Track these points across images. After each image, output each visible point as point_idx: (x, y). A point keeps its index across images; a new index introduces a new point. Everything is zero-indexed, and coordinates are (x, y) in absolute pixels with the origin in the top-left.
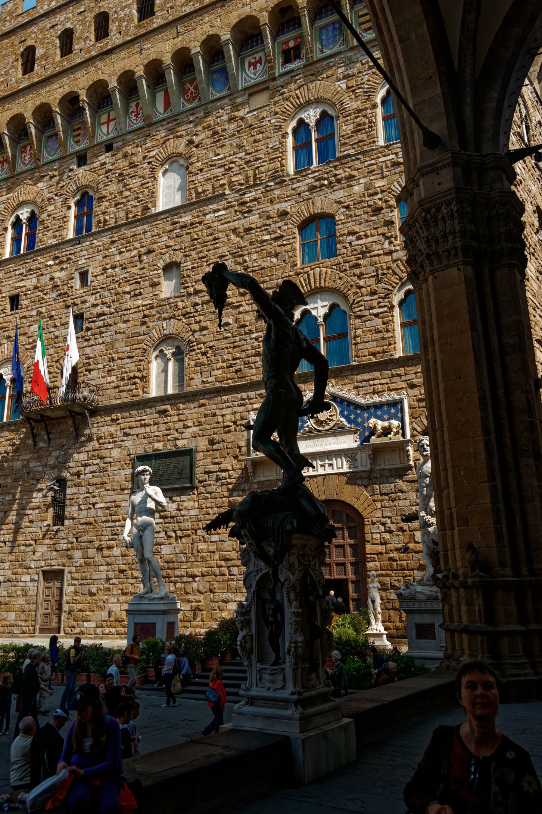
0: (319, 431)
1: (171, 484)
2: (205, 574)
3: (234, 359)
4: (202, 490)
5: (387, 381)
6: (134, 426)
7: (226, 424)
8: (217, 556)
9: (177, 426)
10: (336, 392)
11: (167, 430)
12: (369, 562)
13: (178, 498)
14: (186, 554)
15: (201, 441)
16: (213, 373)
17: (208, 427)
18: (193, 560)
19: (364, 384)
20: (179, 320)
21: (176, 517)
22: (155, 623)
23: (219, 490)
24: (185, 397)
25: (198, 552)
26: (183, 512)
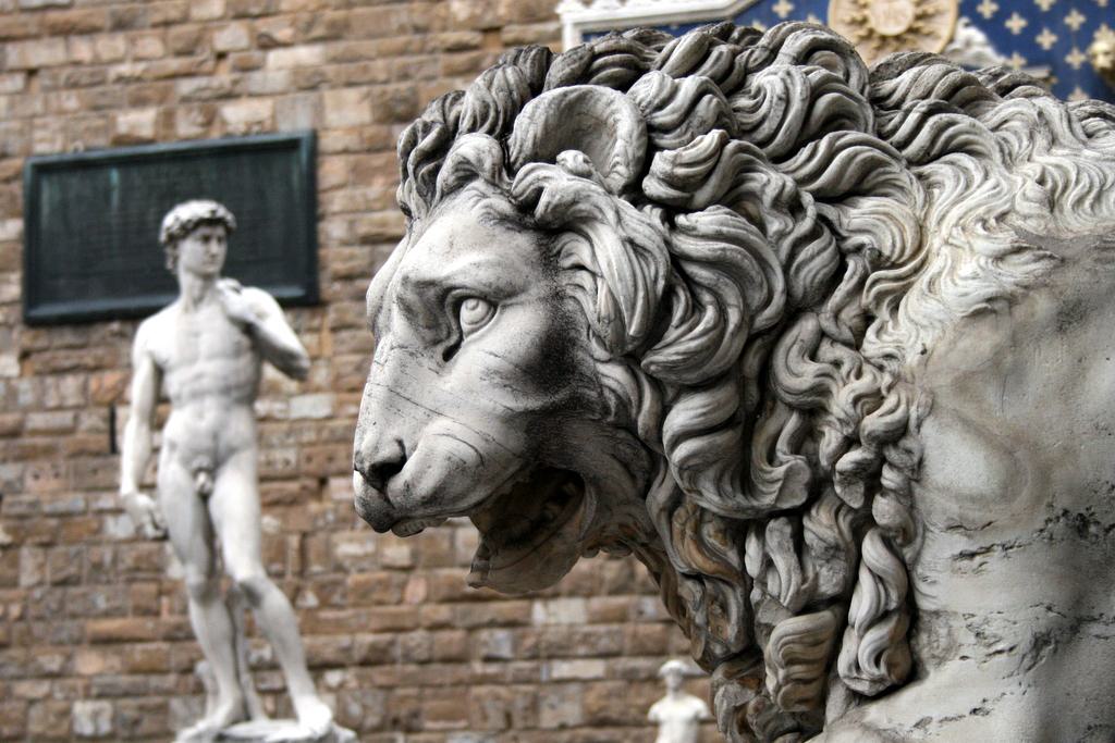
6: (19, 31)
11: (179, 54)
15: (339, 106)
17: (368, 47)
25: (340, 568)
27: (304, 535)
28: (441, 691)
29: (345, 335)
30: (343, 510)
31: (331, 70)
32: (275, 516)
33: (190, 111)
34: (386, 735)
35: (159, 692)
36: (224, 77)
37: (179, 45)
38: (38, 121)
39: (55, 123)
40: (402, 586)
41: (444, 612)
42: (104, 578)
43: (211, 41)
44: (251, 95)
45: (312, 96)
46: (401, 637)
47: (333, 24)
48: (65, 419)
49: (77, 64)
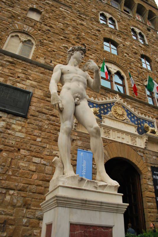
0: (116, 118)
1: (5, 107)
4: (33, 121)
5: (146, 111)
9: (20, 75)
12: (148, 202)
13: (8, 120)
14: (4, 166)
15: (38, 91)
16: (53, 62)
18: (10, 173)
19: (137, 108)
20: (36, 30)
22: (111, 228)
23: (47, 127)
24: (30, 63)
25: (19, 168)
26: (9, 132)
27: (12, 159)
28: (36, 200)
29: (31, 125)
30: (22, 156)
31: (38, 86)
32: (6, 154)
34: (21, 208)
36: (18, 80)
37: (12, 72)
40: (32, 175)
41: (41, 183)
43: (18, 74)
44: (22, 84)
45: (34, 88)
46: (30, 186)
47: (40, 81)
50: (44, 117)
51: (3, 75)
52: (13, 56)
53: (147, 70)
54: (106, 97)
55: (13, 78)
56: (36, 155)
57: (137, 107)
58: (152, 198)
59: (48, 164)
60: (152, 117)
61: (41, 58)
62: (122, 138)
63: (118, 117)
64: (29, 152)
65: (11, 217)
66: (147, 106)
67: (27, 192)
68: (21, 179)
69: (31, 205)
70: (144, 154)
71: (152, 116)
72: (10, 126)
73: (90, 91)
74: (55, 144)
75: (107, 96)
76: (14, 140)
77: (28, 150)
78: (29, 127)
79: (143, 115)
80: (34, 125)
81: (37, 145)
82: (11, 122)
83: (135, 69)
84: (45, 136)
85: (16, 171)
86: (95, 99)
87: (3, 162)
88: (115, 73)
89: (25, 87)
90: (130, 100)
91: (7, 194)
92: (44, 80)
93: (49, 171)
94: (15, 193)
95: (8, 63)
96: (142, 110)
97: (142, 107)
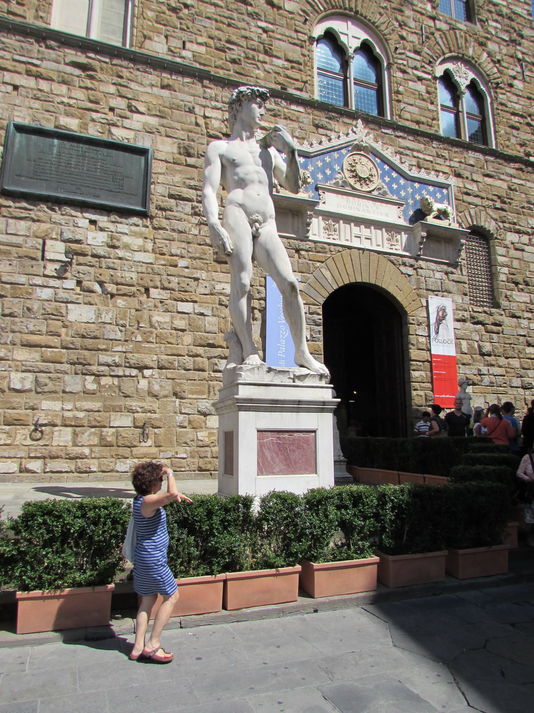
0: (354, 188)
1: (98, 197)
2: (167, 365)
3: (229, 42)
4: (164, 223)
6: (10, 68)
7: (212, 132)
8: (188, 338)
10: (378, 149)
11: (91, 101)
12: (414, 370)
13: (112, 227)
14: (123, 326)
15: (163, 143)
16: (188, 45)
18: (139, 338)
19: (408, 152)
21: (105, 257)
23: (197, 232)
24: (131, 60)
25: (152, 326)
26: (120, 253)
31: (162, 129)
33: (96, 126)
35: (57, 371)
37: (92, 98)
38: (16, 108)
39: (25, 112)
42: (33, 316)
43: (107, 102)
48: (19, 240)
49: (41, 90)
50: (187, 207)
51: (72, 110)
52: (84, 45)
53: (450, 24)
54: (329, 133)
55: (99, 115)
56: (183, 297)
57: (409, 149)
58: (423, 362)
59: (209, 313)
60: (444, 173)
61: (156, 38)
62: (366, 238)
63: (358, 186)
64: (169, 291)
65: (154, 416)
66: (435, 144)
67: (175, 369)
68: (160, 347)
69: (187, 391)
70: (415, 269)
71: (447, 170)
72: (118, 240)
73: (289, 122)
74: (219, 270)
75: (331, 130)
76: (133, 270)
77: (164, 288)
78: (159, 237)
79: (423, 170)
80: (167, 230)
81: (180, 276)
82: (119, 230)
83: (412, 24)
84: (196, 253)
85: (148, 334)
86: (302, 144)
87: (121, 319)
88: (356, 51)
89: (130, 135)
90: (389, 131)
91: (140, 377)
92: (174, 106)
93: (211, 326)
94: (154, 373)
95: (77, 72)
96: (421, 156)
97: (422, 146)
